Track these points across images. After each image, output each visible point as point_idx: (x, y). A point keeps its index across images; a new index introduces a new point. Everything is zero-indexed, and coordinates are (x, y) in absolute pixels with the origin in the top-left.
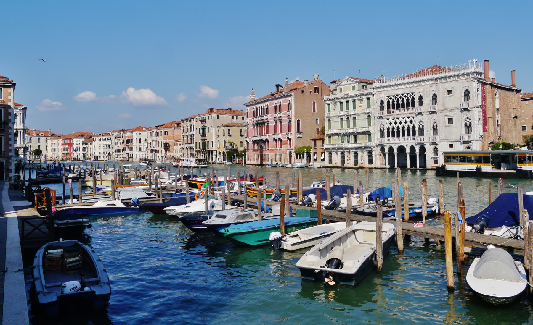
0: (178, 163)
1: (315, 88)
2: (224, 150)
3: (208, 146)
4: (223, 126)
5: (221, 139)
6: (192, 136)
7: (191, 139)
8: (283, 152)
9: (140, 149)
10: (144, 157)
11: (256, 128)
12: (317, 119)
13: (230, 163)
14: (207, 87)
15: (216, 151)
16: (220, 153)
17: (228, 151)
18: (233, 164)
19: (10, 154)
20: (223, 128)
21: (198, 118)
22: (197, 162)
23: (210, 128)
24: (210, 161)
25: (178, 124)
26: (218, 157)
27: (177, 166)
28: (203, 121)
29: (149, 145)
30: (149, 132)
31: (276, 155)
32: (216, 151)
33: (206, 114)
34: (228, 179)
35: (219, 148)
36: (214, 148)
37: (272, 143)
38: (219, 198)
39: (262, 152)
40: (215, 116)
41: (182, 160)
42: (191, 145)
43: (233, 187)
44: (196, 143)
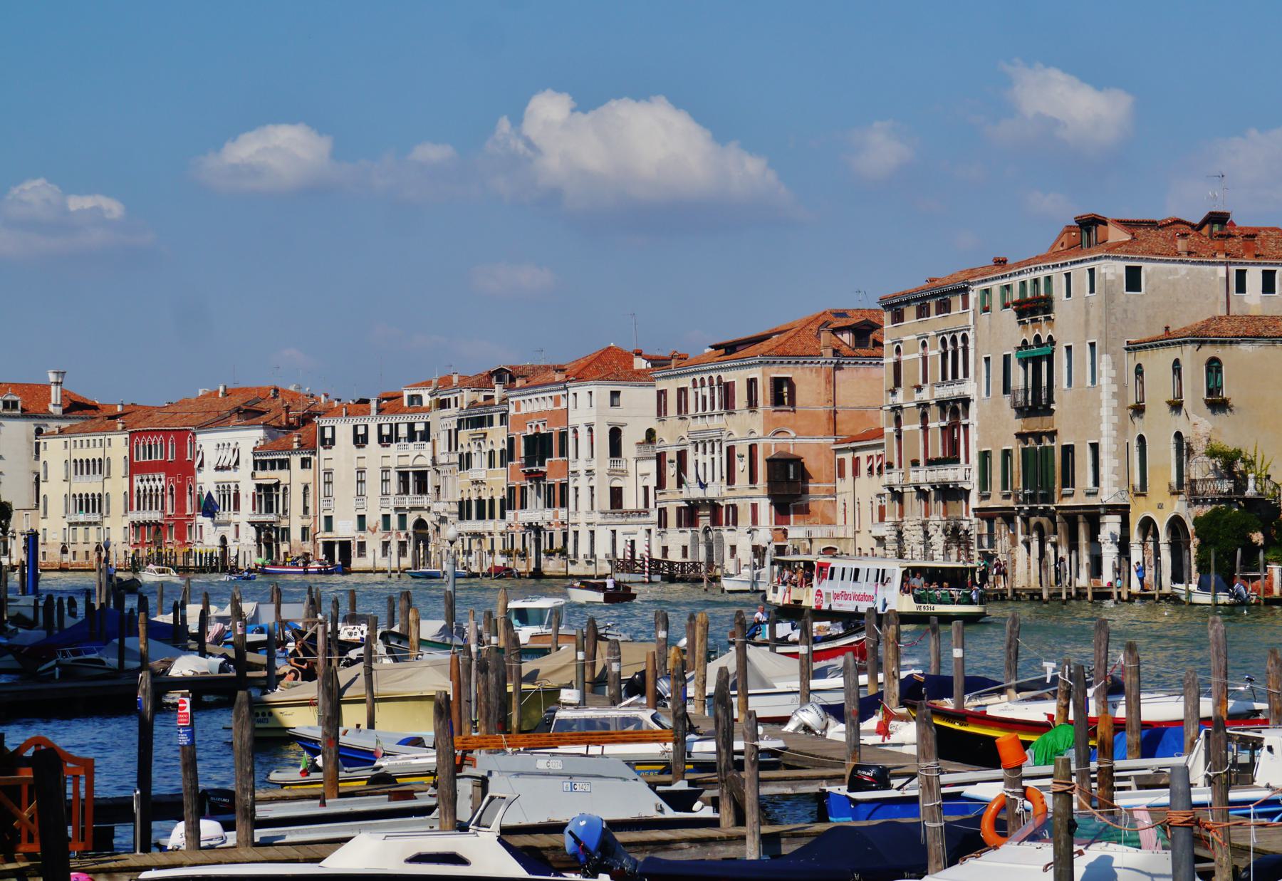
0: (797, 593)
3: (1068, 480)
4: (1168, 340)
5: (1160, 428)
6: (956, 408)
7: (948, 431)
9: (616, 494)
10: (640, 550)
13: (1223, 598)
14: (1055, 74)
15: (1123, 511)
16: (1148, 525)
18: (1241, 602)
20: (1175, 353)
21: (995, 286)
22: (918, 582)
24: (1083, 581)
26: (1136, 555)
27: (793, 612)
28: (1034, 307)
29: (671, 470)
30: (671, 386)
32: (1123, 511)
33: (1052, 257)
34: (1207, 707)
35: (1142, 491)
36: (1108, 494)
38: (1149, 835)
40: (1112, 270)
41: (826, 572)
42: (949, 474)
43: (1250, 767)
44: (985, 456)
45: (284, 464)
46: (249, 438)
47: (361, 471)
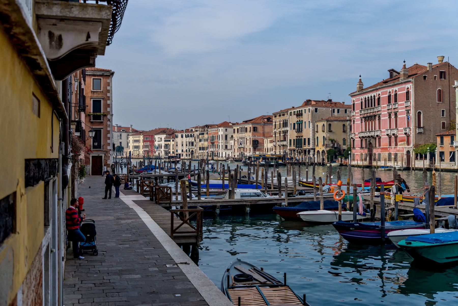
1: (441, 73)
2: (323, 148)
3: (305, 144)
4: (322, 120)
8: (399, 151)
11: (364, 123)
12: (443, 111)
16: (318, 152)
17: (328, 149)
19: (109, 148)
20: (323, 123)
23: (307, 123)
25: (269, 119)
28: (299, 114)
31: (390, 155)
32: (314, 149)
37: (385, 141)
39: (370, 150)
42: (285, 143)
45: (170, 141)
46: (163, 136)
47: (182, 142)
